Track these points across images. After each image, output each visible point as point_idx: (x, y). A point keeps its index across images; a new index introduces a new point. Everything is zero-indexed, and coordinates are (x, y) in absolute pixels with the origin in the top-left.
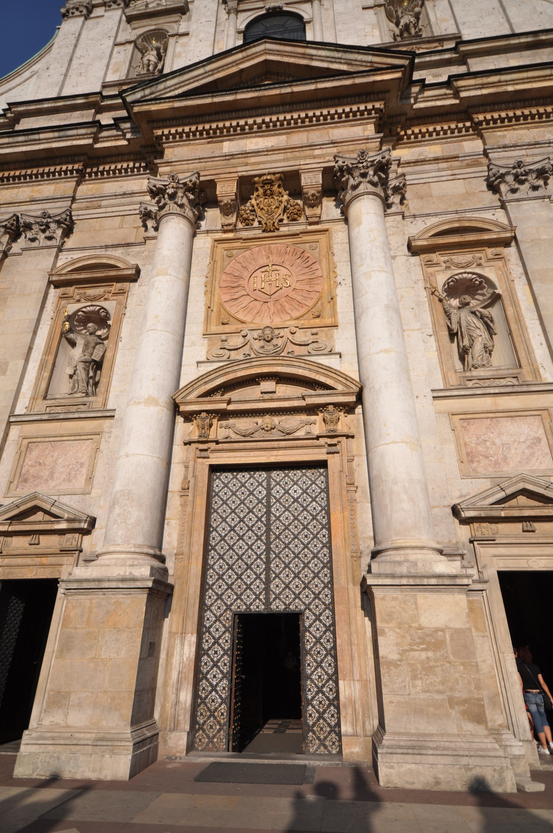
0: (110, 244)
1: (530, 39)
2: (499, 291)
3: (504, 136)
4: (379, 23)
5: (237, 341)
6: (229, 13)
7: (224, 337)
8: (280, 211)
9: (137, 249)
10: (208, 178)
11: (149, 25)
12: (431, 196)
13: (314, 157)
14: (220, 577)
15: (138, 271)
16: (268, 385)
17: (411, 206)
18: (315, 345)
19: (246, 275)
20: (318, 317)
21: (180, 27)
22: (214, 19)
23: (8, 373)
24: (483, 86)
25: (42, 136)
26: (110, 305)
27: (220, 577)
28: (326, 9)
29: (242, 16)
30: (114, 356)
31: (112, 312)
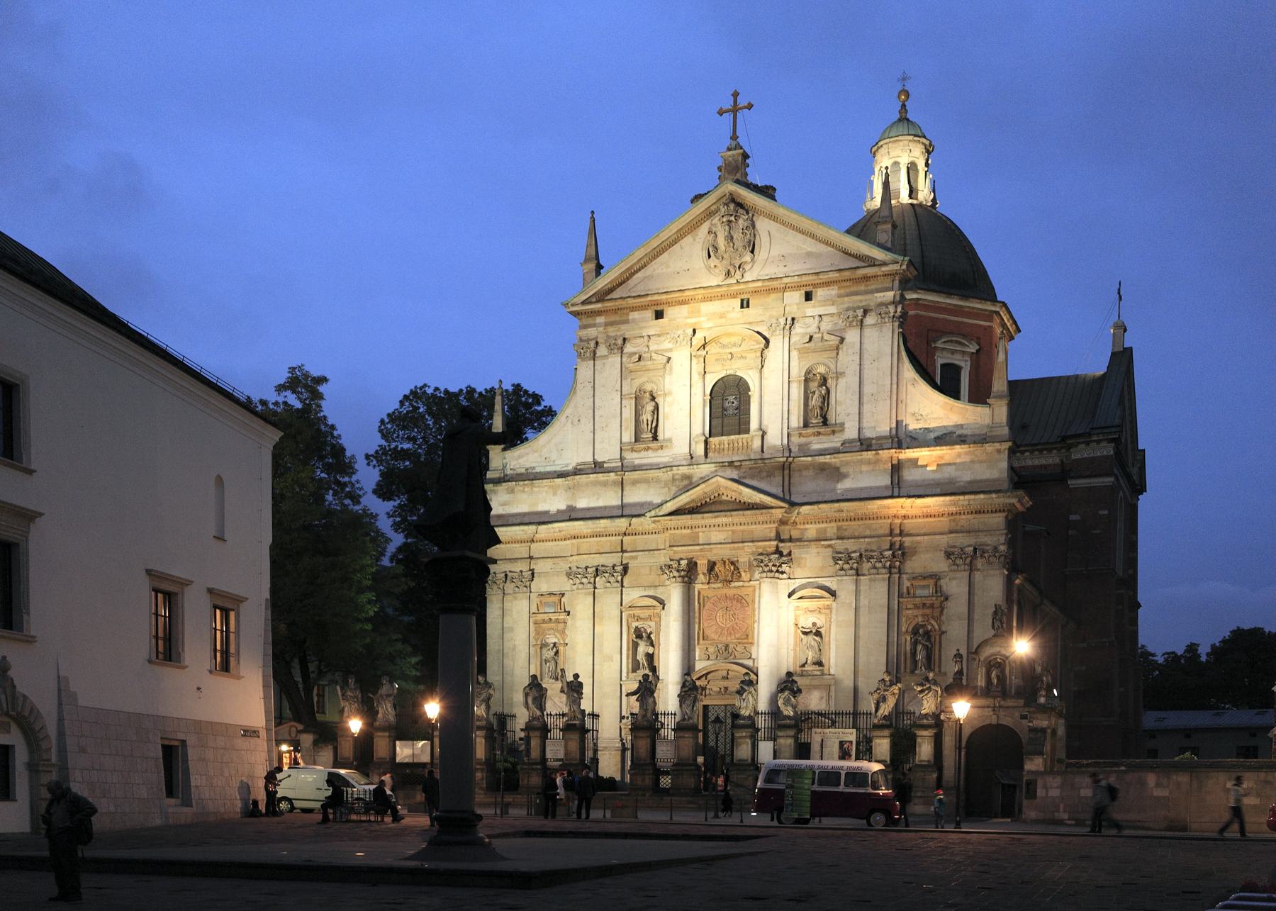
29: (707, 376)
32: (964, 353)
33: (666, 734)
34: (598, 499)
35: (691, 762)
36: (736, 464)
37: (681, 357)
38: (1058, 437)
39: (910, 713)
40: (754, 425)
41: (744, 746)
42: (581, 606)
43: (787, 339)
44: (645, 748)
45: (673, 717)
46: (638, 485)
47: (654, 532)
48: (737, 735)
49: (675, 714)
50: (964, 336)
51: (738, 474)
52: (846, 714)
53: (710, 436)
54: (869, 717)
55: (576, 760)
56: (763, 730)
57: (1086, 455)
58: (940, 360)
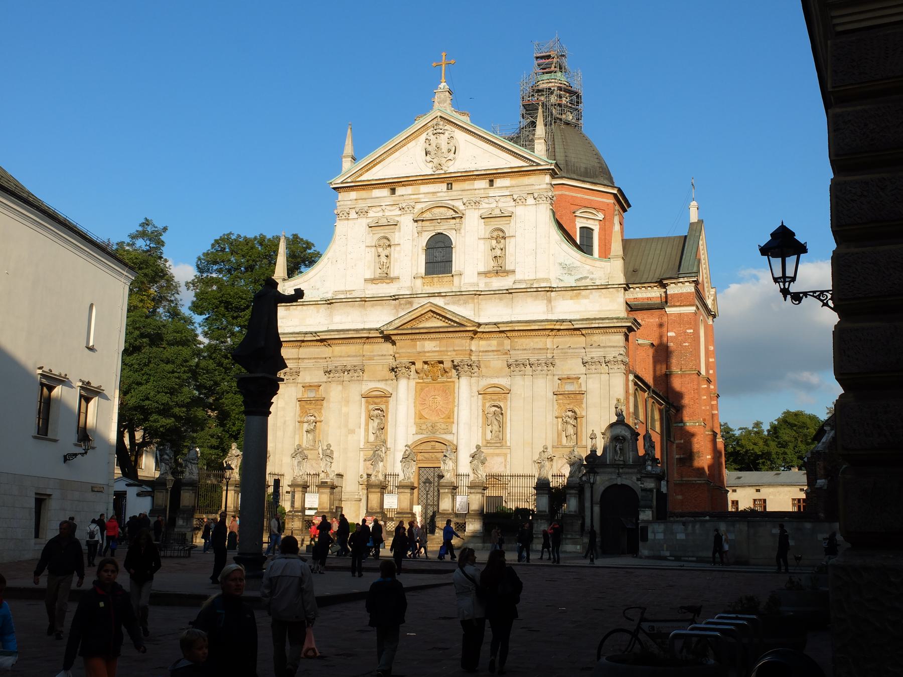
0: (380, 379)
1: (535, 290)
4: (484, 252)
5: (424, 427)
11: (381, 232)
12: (490, 367)
13: (448, 355)
14: (422, 496)
15: (391, 394)
16: (433, 443)
17: (483, 371)
19: (427, 399)
20: (449, 418)
21: (396, 236)
22: (411, 239)
23: (356, 433)
24: (507, 327)
26: (383, 407)
27: (422, 496)
30: (387, 429)
31: (384, 410)
33: (392, 489)
34: (348, 316)
35: (409, 511)
36: (443, 294)
37: (406, 221)
41: (446, 500)
42: (333, 392)
44: (376, 500)
46: (375, 307)
48: (441, 491)
49: (398, 475)
51: (444, 302)
53: (425, 275)
54: (533, 478)
55: (327, 509)
56: (460, 487)
57: (676, 292)
58: (580, 223)
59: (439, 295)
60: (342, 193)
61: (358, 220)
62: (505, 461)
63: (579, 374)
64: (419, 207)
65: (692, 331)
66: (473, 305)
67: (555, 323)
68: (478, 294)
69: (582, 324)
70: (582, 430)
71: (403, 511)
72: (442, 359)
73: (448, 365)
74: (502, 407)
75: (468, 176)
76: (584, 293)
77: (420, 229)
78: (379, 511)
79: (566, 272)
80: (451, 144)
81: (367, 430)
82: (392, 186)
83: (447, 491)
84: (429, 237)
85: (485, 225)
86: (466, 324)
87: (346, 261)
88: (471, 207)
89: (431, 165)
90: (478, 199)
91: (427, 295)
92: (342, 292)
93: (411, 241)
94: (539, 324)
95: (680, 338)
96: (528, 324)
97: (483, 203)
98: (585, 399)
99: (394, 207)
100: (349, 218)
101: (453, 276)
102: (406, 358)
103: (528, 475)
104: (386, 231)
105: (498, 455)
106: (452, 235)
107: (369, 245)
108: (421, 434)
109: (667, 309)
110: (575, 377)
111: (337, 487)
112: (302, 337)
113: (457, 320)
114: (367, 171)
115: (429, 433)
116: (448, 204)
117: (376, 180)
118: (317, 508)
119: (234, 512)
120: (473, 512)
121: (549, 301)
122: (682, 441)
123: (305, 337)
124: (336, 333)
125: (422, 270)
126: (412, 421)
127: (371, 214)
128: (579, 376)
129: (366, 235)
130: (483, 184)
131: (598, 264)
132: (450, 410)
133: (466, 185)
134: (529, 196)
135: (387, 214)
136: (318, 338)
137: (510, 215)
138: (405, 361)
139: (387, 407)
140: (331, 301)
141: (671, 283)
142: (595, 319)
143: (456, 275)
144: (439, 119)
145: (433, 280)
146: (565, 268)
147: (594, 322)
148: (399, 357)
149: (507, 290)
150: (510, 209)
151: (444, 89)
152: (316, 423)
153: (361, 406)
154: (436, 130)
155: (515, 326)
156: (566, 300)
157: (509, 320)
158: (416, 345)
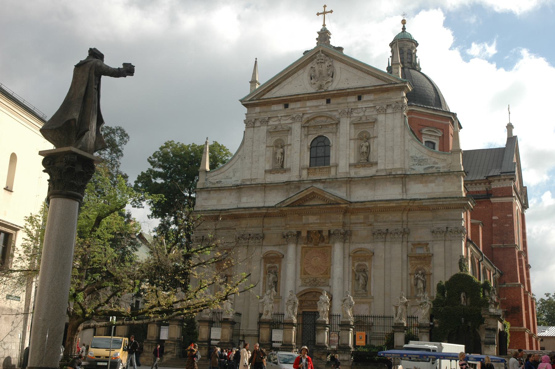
2: (368, 270)
3: (379, 216)
5: (308, 281)
6: (305, 136)
7: (305, 279)
8: (318, 239)
9: (282, 247)
10: (299, 230)
13: (326, 226)
18: (325, 283)
20: (327, 274)
21: (289, 139)
22: (300, 140)
24: (371, 204)
25: (253, 209)
26: (277, 265)
28: (338, 138)
30: (280, 282)
31: (278, 267)
32: (436, 136)
34: (252, 197)
36: (322, 181)
37: (297, 128)
38: (484, 177)
39: (415, 318)
40: (332, 161)
43: (349, 119)
45: (283, 316)
47: (280, 215)
49: (284, 315)
50: (437, 128)
52: (379, 317)
54: (392, 319)
55: (228, 340)
57: (499, 186)
59: (319, 181)
60: (249, 108)
61: (261, 128)
62: (370, 307)
63: (427, 241)
64: (306, 116)
65: (511, 215)
66: (346, 188)
67: (408, 201)
68: (349, 181)
69: (429, 202)
70: (430, 284)
71: (287, 343)
72: (321, 229)
73: (325, 234)
74: (367, 264)
75: (343, 94)
76: (431, 179)
77: (306, 133)
78: (268, 343)
79: (417, 163)
80: (330, 70)
81: (264, 283)
82: (286, 102)
83: (322, 328)
84: (313, 139)
85: (355, 129)
86: (340, 202)
87: (252, 156)
88: (344, 116)
89: (315, 86)
90: (350, 110)
91: (311, 181)
92: (248, 180)
93: (300, 142)
94: (396, 202)
95: (502, 221)
96: (388, 202)
97: (354, 113)
98: (432, 260)
99: (287, 118)
100: (255, 126)
101: (330, 167)
102: (294, 229)
103: (388, 316)
104: (281, 135)
105: (363, 303)
106: (330, 137)
107: (269, 145)
108: (306, 285)
109: (491, 200)
110: (425, 243)
111: (236, 323)
112: (218, 213)
113: (333, 199)
114: (268, 91)
115: (311, 285)
116: (327, 114)
117: (274, 98)
118: (220, 339)
119: (156, 341)
120: (343, 346)
121: (404, 185)
122: (505, 299)
123: (220, 213)
124: (243, 210)
125: (307, 162)
126: (298, 276)
127: (271, 123)
128: (428, 242)
129: (267, 138)
130: (353, 99)
131: (441, 157)
132: (327, 268)
133: (340, 100)
134: (388, 107)
135: (282, 123)
136: (230, 213)
137: (374, 121)
138: (294, 230)
139: (280, 265)
140: (240, 187)
141: (494, 180)
142: (440, 198)
143: (333, 166)
144: (321, 52)
145: (315, 171)
146: (416, 160)
147: (439, 200)
148: (289, 228)
149: (372, 176)
150: (374, 117)
151: (325, 30)
152: (227, 277)
153: (261, 265)
154: (318, 60)
155: (378, 204)
156: (417, 183)
157: (373, 199)
158: (302, 219)
